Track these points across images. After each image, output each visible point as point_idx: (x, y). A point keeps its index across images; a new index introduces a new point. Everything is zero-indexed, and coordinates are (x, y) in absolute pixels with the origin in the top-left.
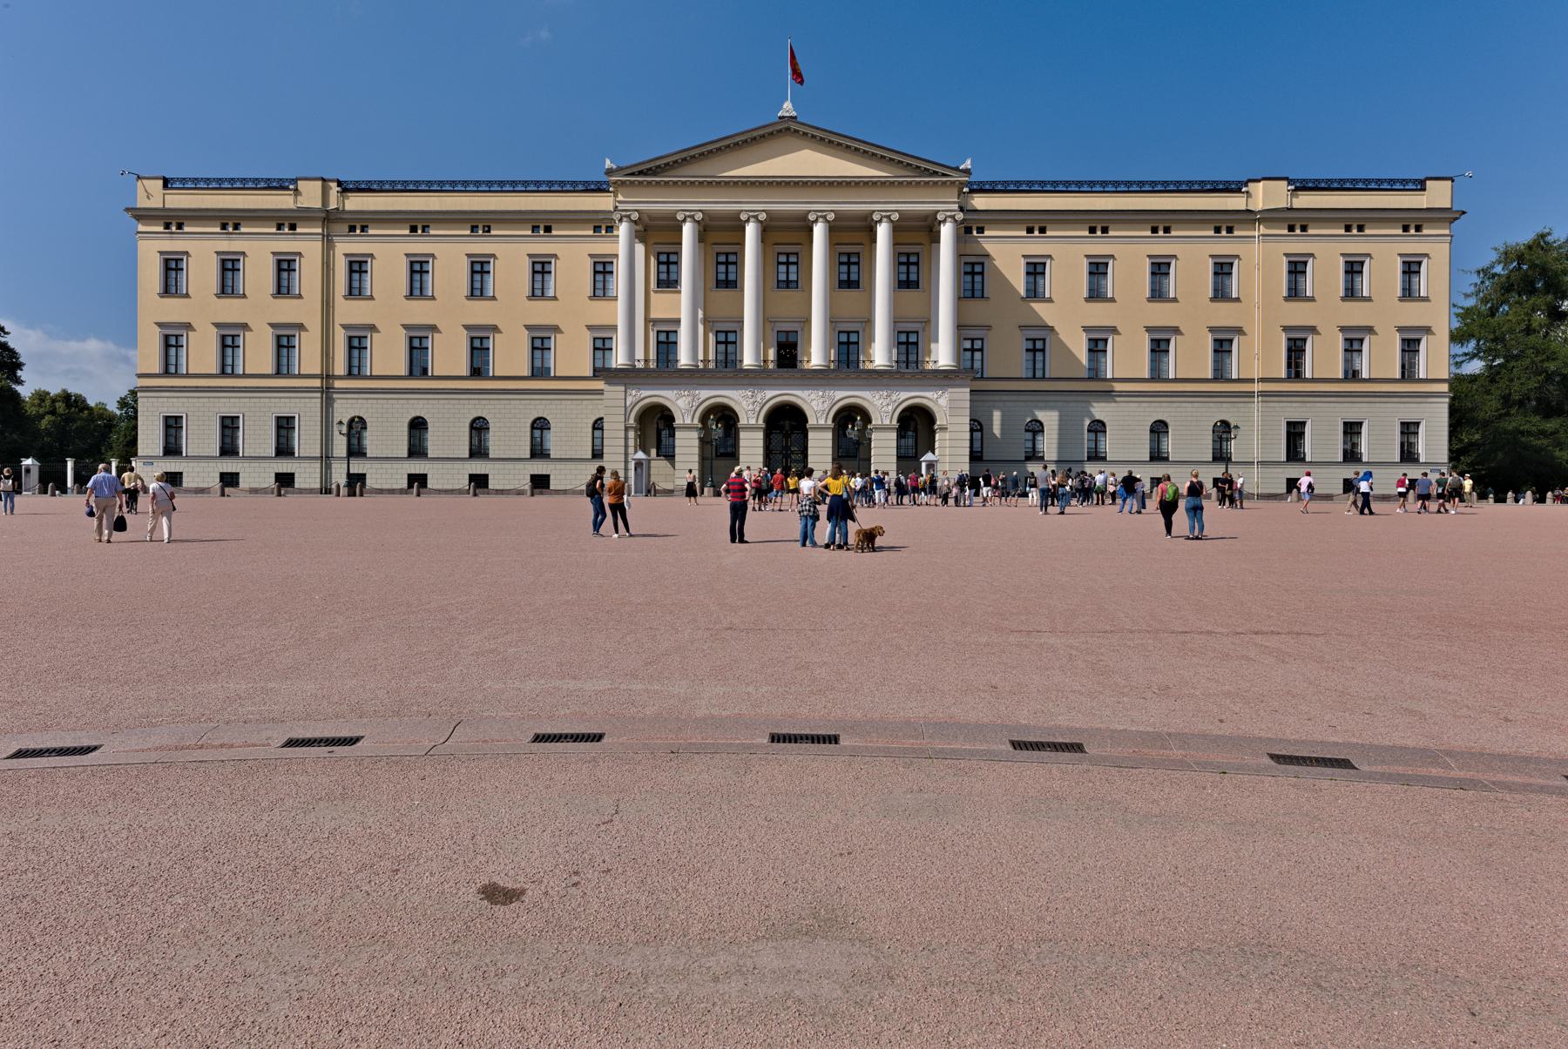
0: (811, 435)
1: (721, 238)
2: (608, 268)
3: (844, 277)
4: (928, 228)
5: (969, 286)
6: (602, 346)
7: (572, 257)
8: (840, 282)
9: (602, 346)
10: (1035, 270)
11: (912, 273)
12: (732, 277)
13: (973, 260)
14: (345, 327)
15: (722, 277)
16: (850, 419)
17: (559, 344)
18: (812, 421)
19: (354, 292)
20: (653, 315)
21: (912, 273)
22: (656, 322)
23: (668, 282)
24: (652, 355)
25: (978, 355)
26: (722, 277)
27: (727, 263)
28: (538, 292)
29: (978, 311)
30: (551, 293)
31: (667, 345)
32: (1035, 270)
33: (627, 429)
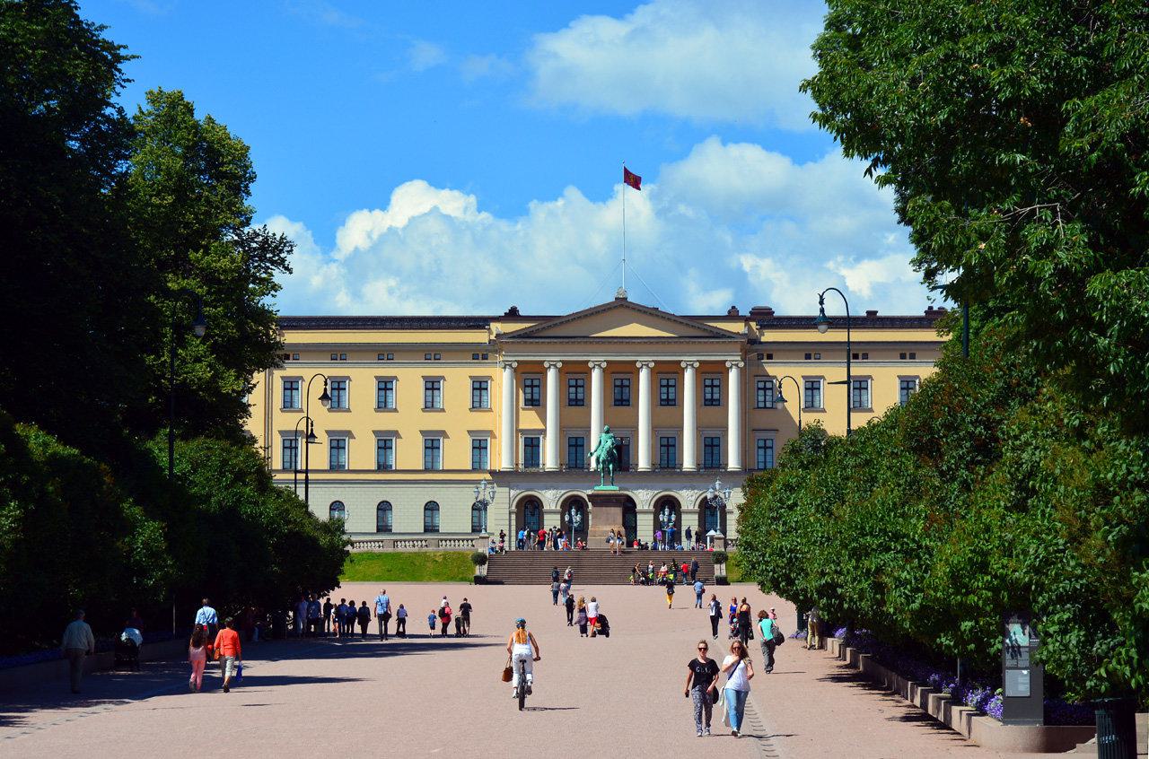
0: (639, 516)
1: (575, 380)
2: (484, 386)
3: (664, 397)
4: (720, 370)
5: (761, 398)
6: (479, 447)
7: (457, 379)
8: (662, 400)
9: (479, 447)
10: (812, 386)
11: (711, 398)
12: (580, 396)
13: (764, 379)
14: (280, 432)
15: (573, 396)
16: (669, 503)
17: (445, 445)
18: (639, 508)
19: (288, 405)
20: (520, 427)
21: (711, 398)
22: (523, 432)
23: (535, 402)
24: (521, 460)
25: (769, 451)
26: (573, 396)
27: (576, 386)
28: (429, 404)
29: (763, 419)
30: (439, 405)
31: (532, 444)
32: (812, 386)
33: (510, 513)
